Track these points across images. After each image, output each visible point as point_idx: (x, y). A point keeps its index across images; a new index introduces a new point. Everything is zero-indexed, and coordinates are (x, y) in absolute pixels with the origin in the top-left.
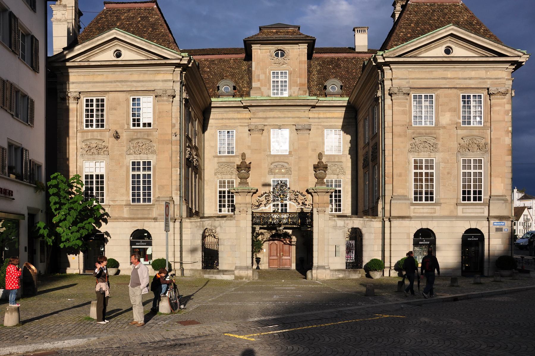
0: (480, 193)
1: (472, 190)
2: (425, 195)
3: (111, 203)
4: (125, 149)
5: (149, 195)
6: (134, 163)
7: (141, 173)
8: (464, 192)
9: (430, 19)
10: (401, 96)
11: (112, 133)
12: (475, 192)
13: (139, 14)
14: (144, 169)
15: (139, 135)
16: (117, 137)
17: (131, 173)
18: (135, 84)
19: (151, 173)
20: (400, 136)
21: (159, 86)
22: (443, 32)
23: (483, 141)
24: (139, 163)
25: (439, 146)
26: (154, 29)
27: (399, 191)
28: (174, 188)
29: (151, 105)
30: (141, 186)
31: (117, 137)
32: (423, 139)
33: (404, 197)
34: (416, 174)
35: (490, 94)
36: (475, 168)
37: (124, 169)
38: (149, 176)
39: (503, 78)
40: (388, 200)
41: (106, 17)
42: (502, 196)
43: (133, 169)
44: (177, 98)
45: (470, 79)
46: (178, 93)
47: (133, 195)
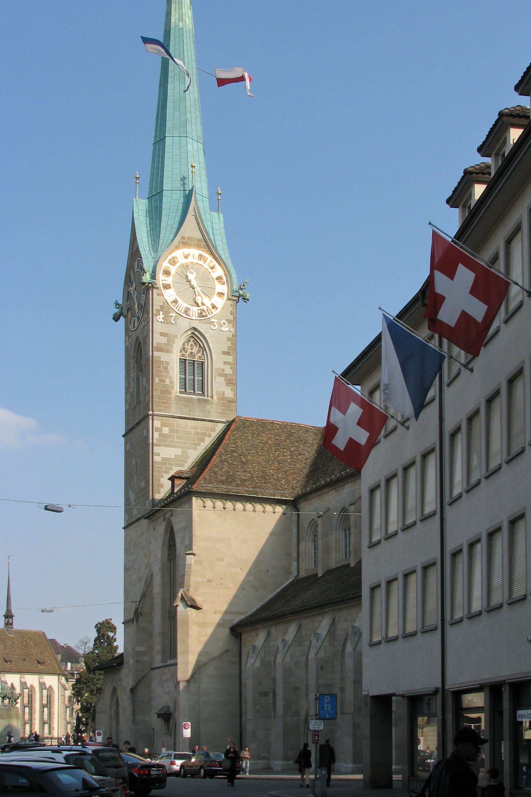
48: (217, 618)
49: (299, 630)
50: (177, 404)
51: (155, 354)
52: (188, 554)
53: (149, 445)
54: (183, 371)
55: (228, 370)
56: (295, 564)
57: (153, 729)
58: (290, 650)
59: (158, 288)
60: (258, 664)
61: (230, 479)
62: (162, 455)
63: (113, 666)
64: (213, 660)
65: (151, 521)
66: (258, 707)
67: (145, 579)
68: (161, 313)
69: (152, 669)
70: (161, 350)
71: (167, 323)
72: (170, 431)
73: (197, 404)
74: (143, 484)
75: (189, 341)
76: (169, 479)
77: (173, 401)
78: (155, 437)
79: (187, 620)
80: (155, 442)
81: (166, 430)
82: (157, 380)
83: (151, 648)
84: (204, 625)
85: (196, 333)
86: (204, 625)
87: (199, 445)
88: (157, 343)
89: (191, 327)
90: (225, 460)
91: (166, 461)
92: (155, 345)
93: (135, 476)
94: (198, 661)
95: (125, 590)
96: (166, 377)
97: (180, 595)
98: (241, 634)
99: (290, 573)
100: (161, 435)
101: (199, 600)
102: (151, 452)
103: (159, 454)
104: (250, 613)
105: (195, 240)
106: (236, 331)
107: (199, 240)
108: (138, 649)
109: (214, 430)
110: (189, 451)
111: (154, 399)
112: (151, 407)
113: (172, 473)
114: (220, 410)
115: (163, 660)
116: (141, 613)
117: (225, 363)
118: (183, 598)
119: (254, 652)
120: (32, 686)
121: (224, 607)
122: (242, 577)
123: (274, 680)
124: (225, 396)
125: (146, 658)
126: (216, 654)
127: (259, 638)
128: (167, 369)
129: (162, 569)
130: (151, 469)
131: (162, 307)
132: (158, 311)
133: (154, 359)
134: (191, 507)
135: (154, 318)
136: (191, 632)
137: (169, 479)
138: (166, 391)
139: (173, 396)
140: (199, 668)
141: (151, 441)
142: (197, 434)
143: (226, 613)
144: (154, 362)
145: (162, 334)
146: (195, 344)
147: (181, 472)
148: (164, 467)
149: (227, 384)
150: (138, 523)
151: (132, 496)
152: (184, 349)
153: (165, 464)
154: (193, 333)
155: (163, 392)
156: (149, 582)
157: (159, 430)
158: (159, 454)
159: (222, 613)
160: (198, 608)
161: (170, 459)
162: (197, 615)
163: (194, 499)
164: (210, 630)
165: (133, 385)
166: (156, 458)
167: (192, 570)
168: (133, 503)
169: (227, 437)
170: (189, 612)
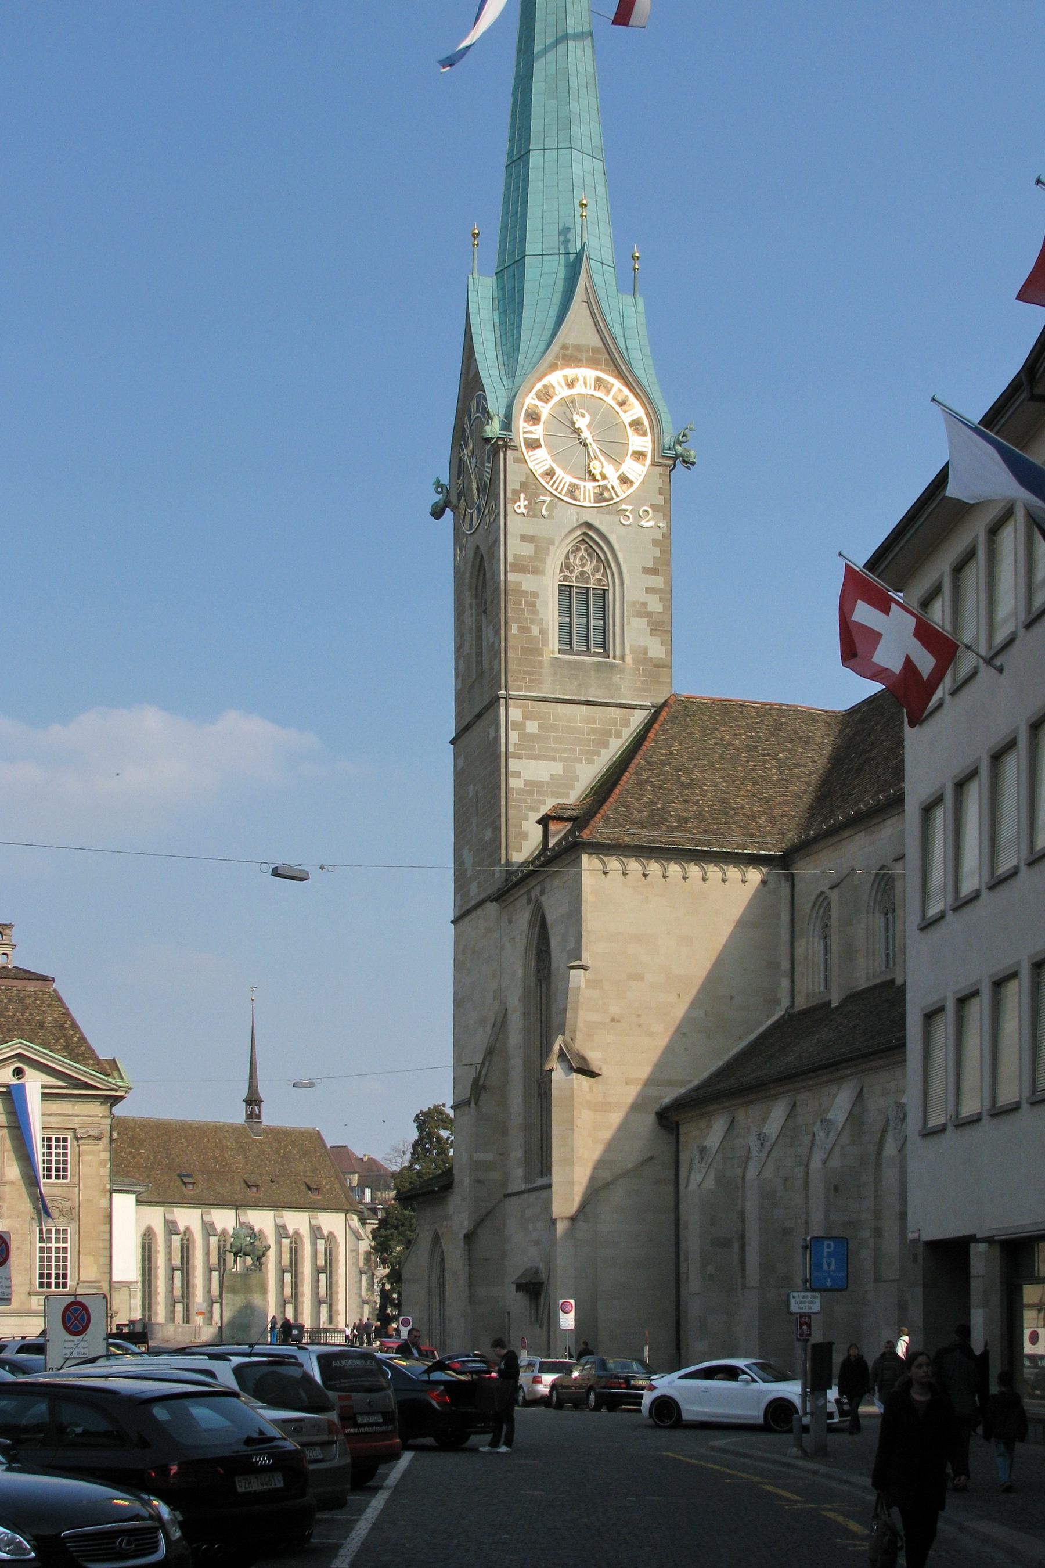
0: (65, 1276)
1: (53, 1272)
8: (41, 1276)
12: (57, 1276)
23: (69, 1204)
35: (77, 1139)
36: (57, 1240)
39: (96, 1116)
42: (94, 1282)
48: (630, 1094)
49: (791, 1115)
50: (555, 674)
51: (511, 577)
52: (572, 968)
53: (499, 756)
54: (566, 609)
55: (655, 605)
56: (785, 983)
57: (509, 1313)
58: (773, 1154)
59: (515, 449)
60: (710, 1184)
61: (657, 818)
62: (526, 776)
63: (433, 1191)
65: (504, 905)
66: (710, 1269)
67: (493, 1020)
68: (522, 496)
69: (506, 1196)
70: (521, 569)
71: (534, 516)
72: (540, 726)
73: (593, 673)
74: (488, 834)
75: (578, 549)
76: (539, 822)
77: (546, 669)
78: (510, 741)
79: (571, 1098)
80: (511, 749)
81: (532, 727)
82: (514, 629)
83: (504, 1154)
84: (604, 1107)
85: (590, 533)
86: (604, 1107)
87: (599, 754)
88: (515, 556)
89: (582, 521)
90: (647, 781)
91: (532, 786)
92: (510, 559)
93: (474, 820)
94: (593, 1179)
95: (456, 1043)
96: (532, 621)
97: (556, 1048)
98: (677, 1124)
99: (777, 1002)
100: (524, 736)
101: (595, 1058)
102: (503, 770)
103: (518, 775)
104: (696, 1082)
105: (588, 351)
106: (669, 527)
107: (596, 350)
108: (479, 1156)
109: (626, 723)
110: (578, 766)
111: (509, 667)
112: (503, 682)
113: (544, 810)
114: (639, 684)
115: (527, 1179)
116: (484, 1087)
117: (648, 590)
118: (562, 1055)
119: (702, 1159)
121: (644, 1072)
122: (679, 1012)
123: (742, 1215)
124: (650, 655)
125: (495, 1176)
126: (630, 1166)
127: (711, 1133)
128: (535, 606)
129: (525, 998)
130: (503, 803)
131: (524, 486)
132: (517, 493)
133: (509, 588)
134: (579, 874)
135: (509, 506)
136: (578, 1122)
137: (539, 822)
138: (534, 650)
139: (546, 658)
140: (595, 1192)
141: (503, 749)
142: (594, 731)
143: (649, 1082)
144: (509, 592)
145: (524, 538)
146: (589, 554)
147: (563, 807)
148: (529, 799)
149: (653, 633)
150: (480, 910)
151: (468, 857)
152: (567, 566)
153: (531, 793)
154: (585, 534)
155: (526, 651)
156: (501, 1026)
157: (520, 726)
158: (518, 775)
159: (641, 1083)
160: (592, 1074)
161: (539, 784)
162: (591, 1089)
163: (585, 857)
164: (616, 1118)
165: (469, 639)
166: (514, 783)
167: (581, 999)
168: (469, 873)
169: (651, 735)
170: (575, 1082)
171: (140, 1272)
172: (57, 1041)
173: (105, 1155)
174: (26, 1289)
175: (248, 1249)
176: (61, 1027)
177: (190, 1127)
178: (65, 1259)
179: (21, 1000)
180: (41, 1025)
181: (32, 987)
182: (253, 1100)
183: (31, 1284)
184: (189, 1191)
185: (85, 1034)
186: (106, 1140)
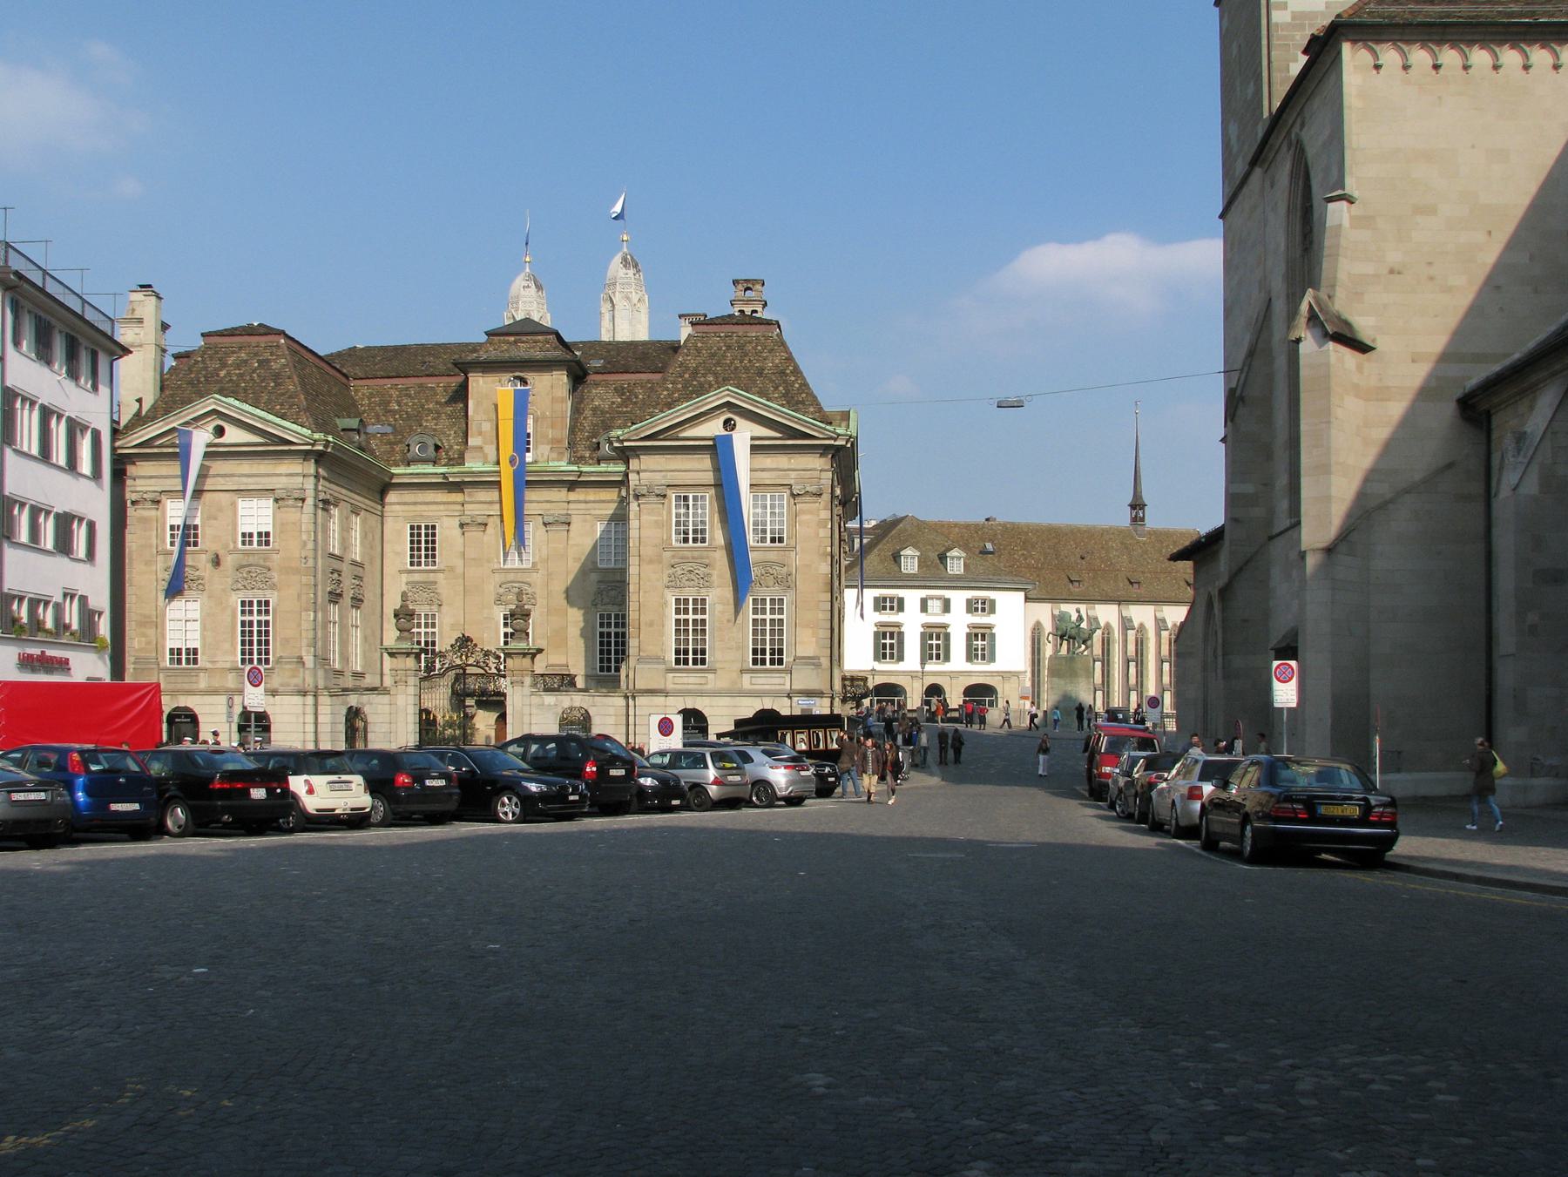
0: (781, 651)
2: (691, 656)
3: (209, 666)
4: (230, 580)
5: (267, 653)
6: (243, 603)
7: (255, 618)
8: (755, 651)
9: (718, 364)
10: (653, 499)
11: (210, 556)
13: (256, 354)
14: (259, 612)
15: (251, 560)
16: (217, 562)
17: (240, 618)
18: (245, 480)
19: (270, 618)
20: (651, 562)
21: (279, 483)
22: (714, 399)
24: (251, 603)
25: (715, 578)
26: (277, 384)
27: (650, 649)
28: (304, 642)
29: (270, 512)
30: (255, 638)
31: (217, 562)
32: (687, 567)
33: (660, 660)
34: (678, 621)
35: (793, 496)
37: (229, 612)
38: (267, 623)
40: (632, 661)
41: (203, 361)
43: (243, 612)
44: (310, 501)
45: (763, 470)
46: (310, 494)
47: (243, 653)
48: (1417, 375)
60: (1531, 486)
64: (1407, 491)
66: (1532, 617)
79: (1328, 376)
83: (1268, 484)
84: (1380, 394)
86: (1380, 394)
94: (1361, 496)
97: (1304, 307)
101: (1364, 326)
116: (1242, 399)
119: (1519, 451)
120: (1142, 625)
121: (1436, 343)
126: (1417, 477)
140: (1365, 514)
143: (1445, 358)
159: (1434, 358)
160: (1362, 348)
162: (1360, 368)
164: (1396, 409)
167: (1343, 242)
170: (1333, 359)
171: (1029, 663)
172: (776, 388)
173: (826, 514)
174: (738, 666)
175: (1073, 632)
176: (783, 373)
177: (1079, 530)
178: (781, 632)
179: (741, 347)
180: (760, 372)
181: (753, 332)
182: (1137, 505)
183: (744, 661)
184: (1075, 589)
185: (809, 380)
186: (826, 497)
